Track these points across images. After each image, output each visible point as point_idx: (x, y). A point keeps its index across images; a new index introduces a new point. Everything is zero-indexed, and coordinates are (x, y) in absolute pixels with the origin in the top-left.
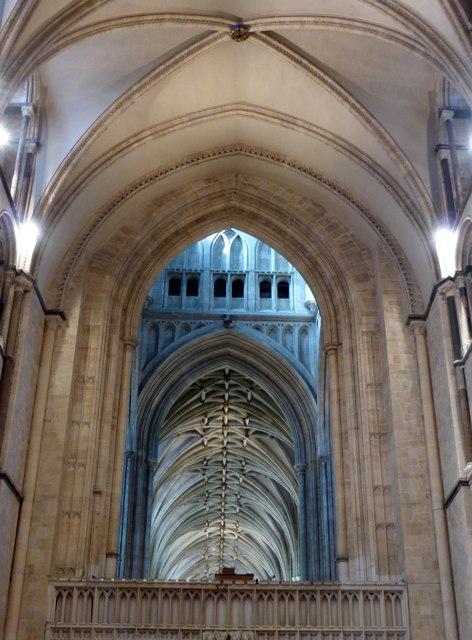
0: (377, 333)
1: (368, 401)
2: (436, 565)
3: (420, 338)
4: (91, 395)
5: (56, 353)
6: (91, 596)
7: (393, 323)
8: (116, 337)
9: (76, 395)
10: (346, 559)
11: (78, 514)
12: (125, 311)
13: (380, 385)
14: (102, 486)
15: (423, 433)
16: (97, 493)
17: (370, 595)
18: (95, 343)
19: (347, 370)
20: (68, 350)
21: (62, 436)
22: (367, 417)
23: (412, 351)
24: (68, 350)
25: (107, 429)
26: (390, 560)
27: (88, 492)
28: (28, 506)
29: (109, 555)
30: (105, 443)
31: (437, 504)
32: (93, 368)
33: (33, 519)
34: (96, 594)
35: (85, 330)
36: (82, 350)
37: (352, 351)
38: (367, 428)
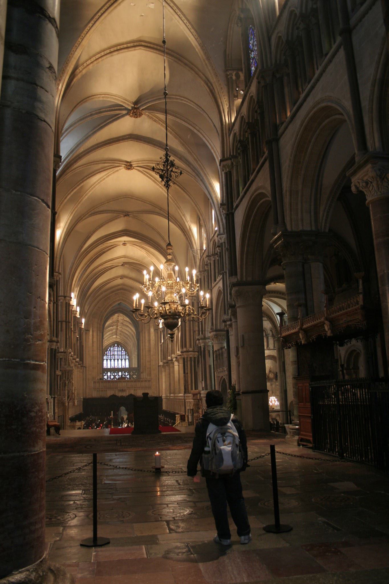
0: (149, 330)
1: (147, 344)
2: (157, 376)
3: (157, 334)
4: (95, 345)
5: (89, 338)
6: (99, 383)
7: (152, 330)
8: (99, 332)
9: (93, 346)
10: (142, 373)
11: (95, 368)
12: (100, 324)
13: (149, 341)
14: (99, 362)
15: (156, 352)
16: (98, 363)
17: (146, 381)
18: (95, 334)
19: (144, 337)
20: (91, 337)
21: (91, 355)
22: (147, 347)
23: (155, 336)
24: (91, 337)
25: (99, 351)
26: (150, 374)
27: (97, 363)
28: (87, 369)
29: (101, 374)
30: (99, 354)
31: (157, 366)
32: (95, 339)
33: (88, 370)
34: (100, 382)
35: (93, 331)
36: (93, 335)
37: (145, 333)
38: (147, 349)
